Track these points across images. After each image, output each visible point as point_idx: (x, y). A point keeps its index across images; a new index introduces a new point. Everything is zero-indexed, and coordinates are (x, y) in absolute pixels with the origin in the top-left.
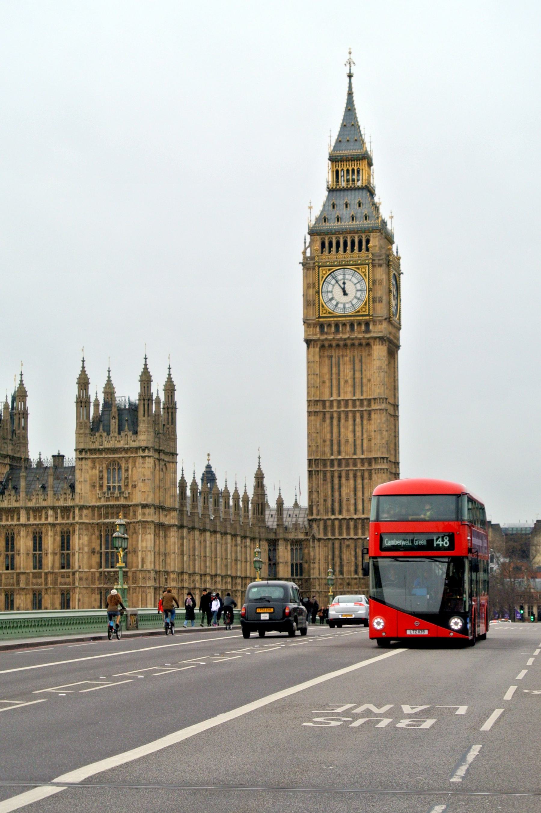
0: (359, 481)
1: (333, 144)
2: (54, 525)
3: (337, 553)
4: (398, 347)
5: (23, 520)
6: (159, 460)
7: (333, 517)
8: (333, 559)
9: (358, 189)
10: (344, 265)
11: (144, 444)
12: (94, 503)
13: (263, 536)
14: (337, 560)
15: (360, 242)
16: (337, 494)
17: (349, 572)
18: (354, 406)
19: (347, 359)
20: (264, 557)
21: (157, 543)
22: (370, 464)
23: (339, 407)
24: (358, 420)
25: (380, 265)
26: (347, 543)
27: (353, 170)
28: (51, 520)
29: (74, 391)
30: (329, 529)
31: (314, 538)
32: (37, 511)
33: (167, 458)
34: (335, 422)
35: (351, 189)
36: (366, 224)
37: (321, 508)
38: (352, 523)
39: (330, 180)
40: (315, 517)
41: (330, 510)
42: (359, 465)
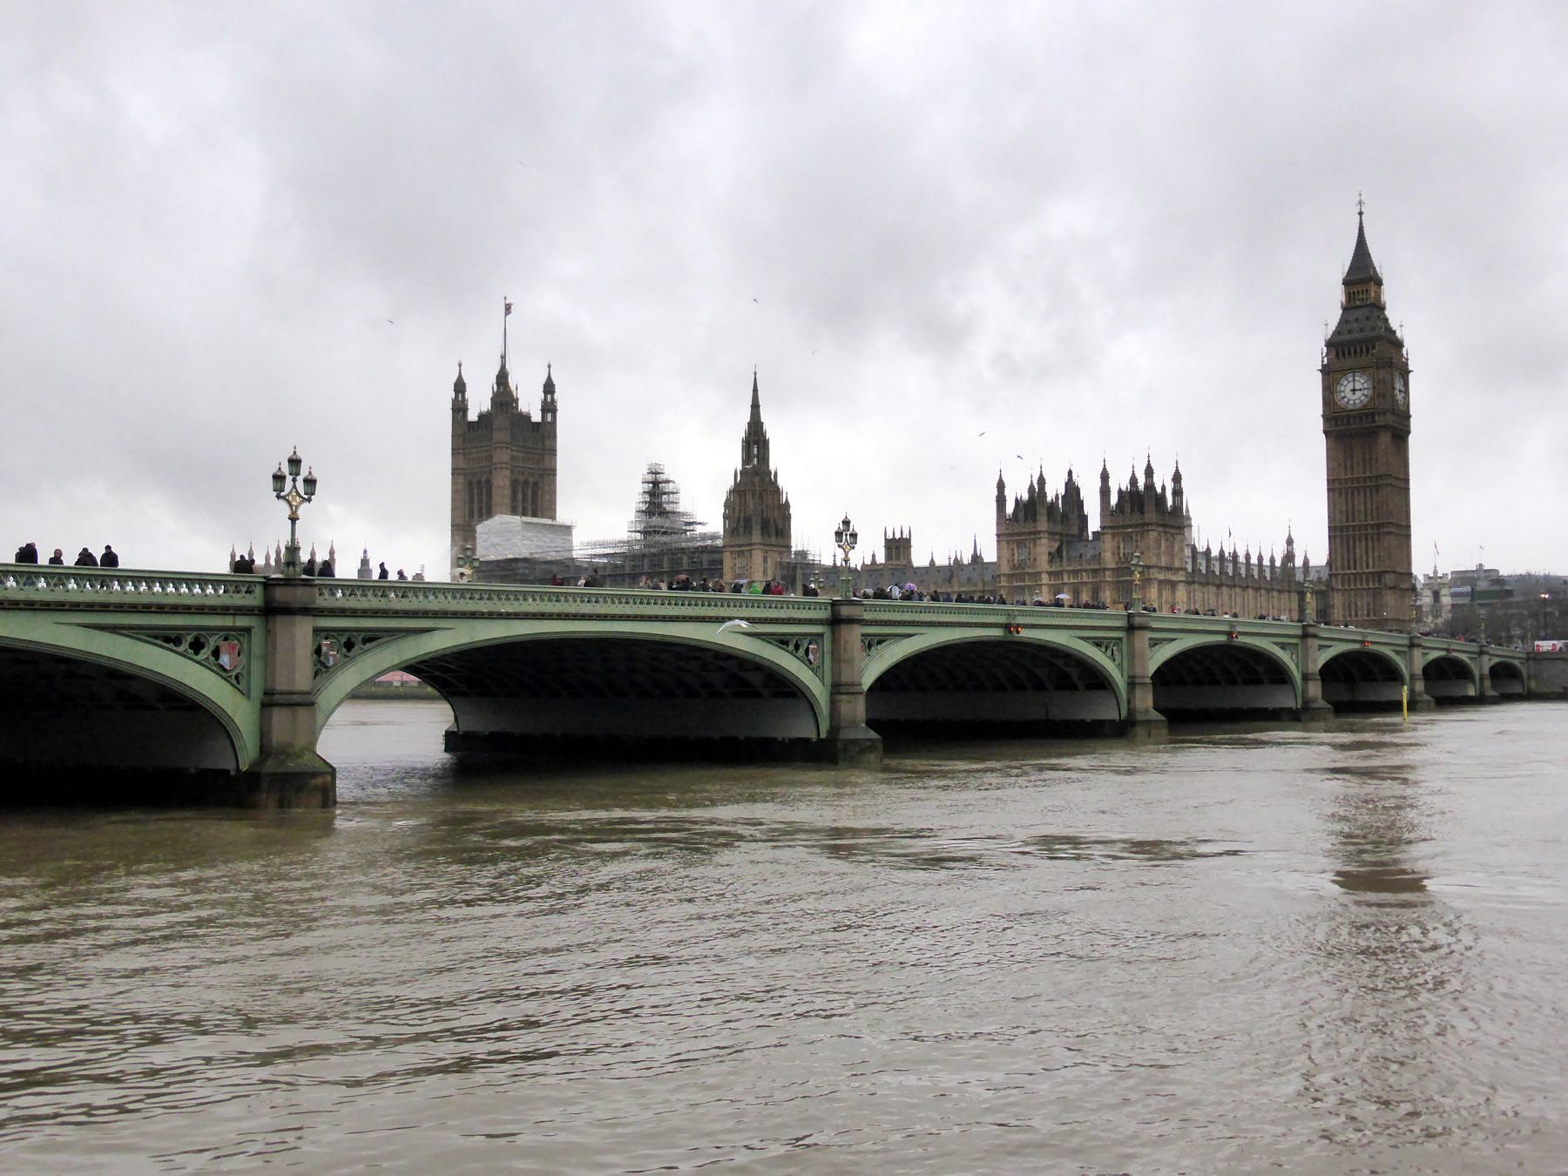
0: (1370, 541)
1: (1346, 271)
2: (1086, 583)
4: (1409, 432)
5: (1066, 580)
6: (1165, 533)
9: (1367, 305)
10: (1353, 370)
11: (1146, 521)
12: (1113, 566)
14: (1353, 606)
15: (1367, 351)
17: (1363, 615)
18: (1365, 482)
20: (1295, 606)
21: (1164, 594)
22: (1378, 529)
24: (1368, 494)
25: (1383, 367)
28: (1085, 579)
29: (1099, 484)
30: (1346, 581)
31: (1333, 589)
32: (1075, 573)
33: (1172, 531)
34: (1350, 496)
35: (1361, 307)
36: (1374, 334)
37: (1339, 564)
39: (1344, 300)
40: (1334, 572)
42: (1369, 531)
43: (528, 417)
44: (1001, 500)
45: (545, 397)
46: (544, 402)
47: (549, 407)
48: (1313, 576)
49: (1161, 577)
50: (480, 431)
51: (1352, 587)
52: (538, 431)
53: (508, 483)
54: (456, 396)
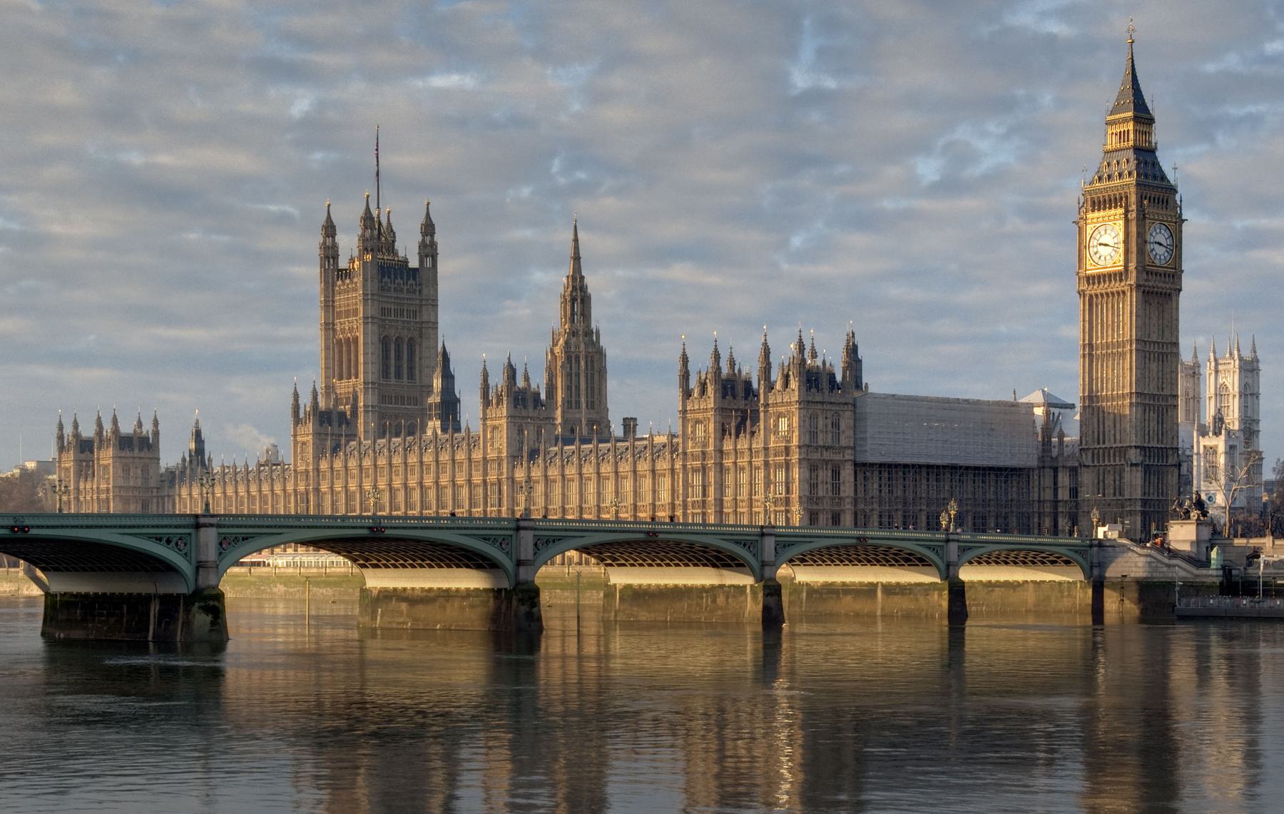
3: (1101, 478)
4: (1180, 290)
7: (1099, 446)
8: (1099, 483)
13: (1047, 464)
14: (1101, 484)
16: (1101, 426)
19: (1110, 305)
20: (1048, 481)
21: (820, 473)
23: (1102, 349)
26: (1108, 468)
27: (1120, 132)
37: (1089, 439)
38: (1112, 452)
40: (1084, 446)
41: (1096, 440)
43: (406, 262)
44: (685, 376)
45: (423, 240)
46: (423, 246)
47: (429, 250)
48: (1067, 451)
49: (816, 456)
50: (348, 281)
51: (1101, 463)
52: (414, 279)
53: (377, 340)
54: (324, 243)
